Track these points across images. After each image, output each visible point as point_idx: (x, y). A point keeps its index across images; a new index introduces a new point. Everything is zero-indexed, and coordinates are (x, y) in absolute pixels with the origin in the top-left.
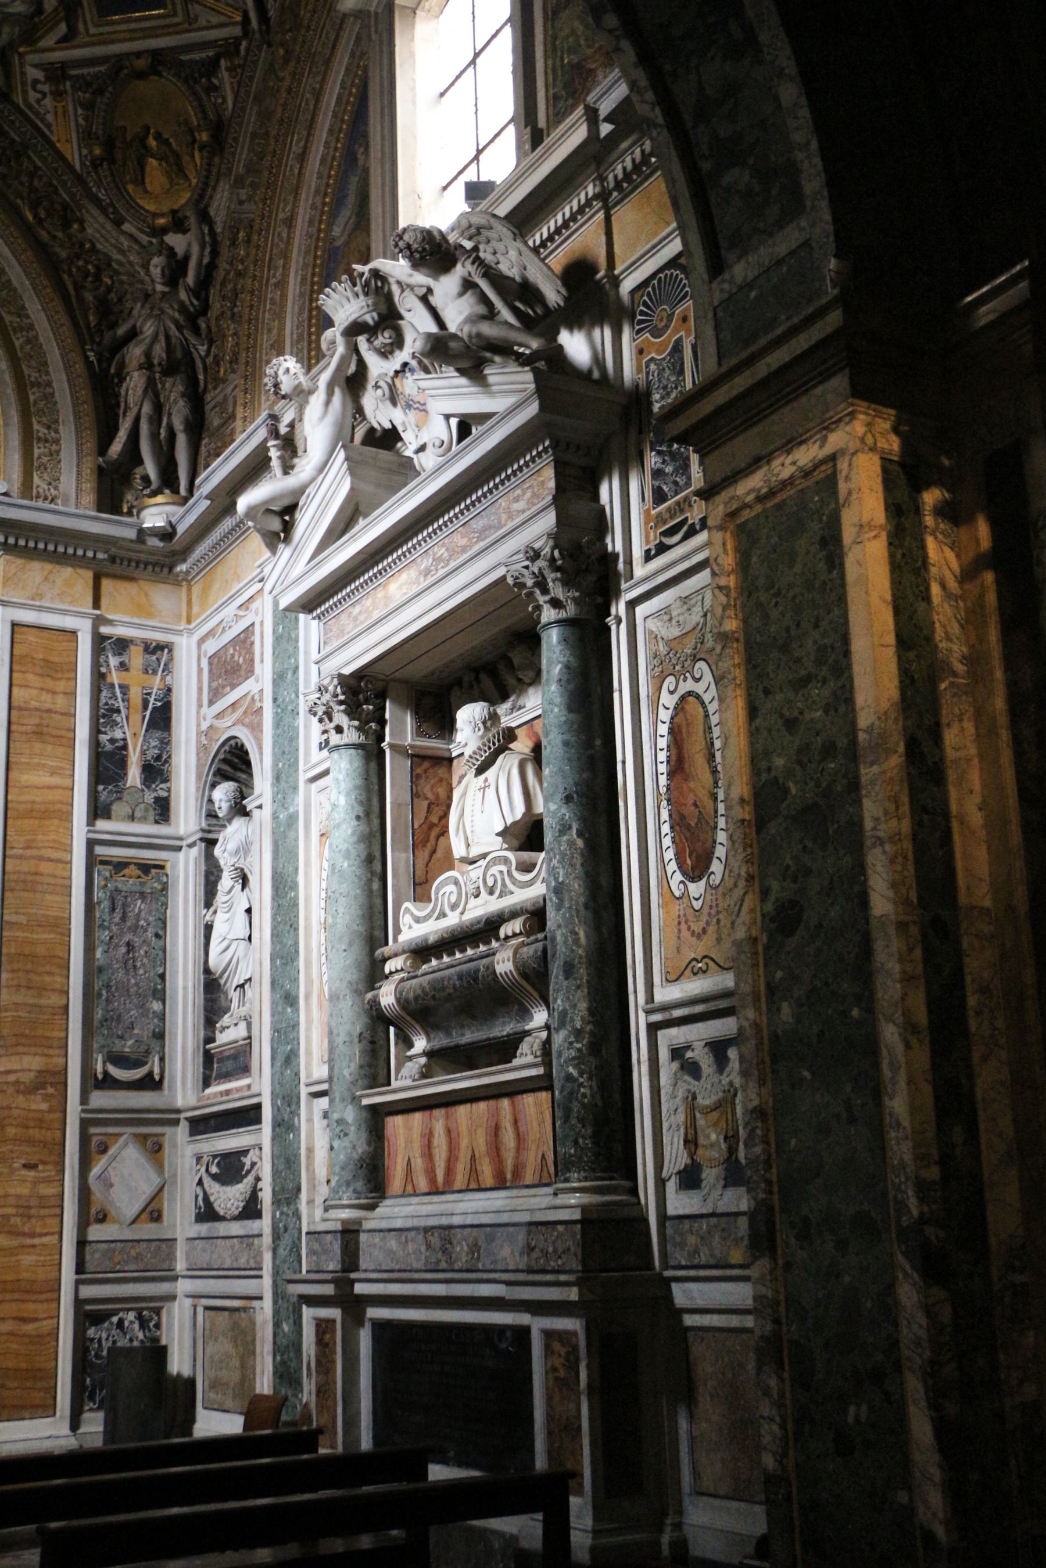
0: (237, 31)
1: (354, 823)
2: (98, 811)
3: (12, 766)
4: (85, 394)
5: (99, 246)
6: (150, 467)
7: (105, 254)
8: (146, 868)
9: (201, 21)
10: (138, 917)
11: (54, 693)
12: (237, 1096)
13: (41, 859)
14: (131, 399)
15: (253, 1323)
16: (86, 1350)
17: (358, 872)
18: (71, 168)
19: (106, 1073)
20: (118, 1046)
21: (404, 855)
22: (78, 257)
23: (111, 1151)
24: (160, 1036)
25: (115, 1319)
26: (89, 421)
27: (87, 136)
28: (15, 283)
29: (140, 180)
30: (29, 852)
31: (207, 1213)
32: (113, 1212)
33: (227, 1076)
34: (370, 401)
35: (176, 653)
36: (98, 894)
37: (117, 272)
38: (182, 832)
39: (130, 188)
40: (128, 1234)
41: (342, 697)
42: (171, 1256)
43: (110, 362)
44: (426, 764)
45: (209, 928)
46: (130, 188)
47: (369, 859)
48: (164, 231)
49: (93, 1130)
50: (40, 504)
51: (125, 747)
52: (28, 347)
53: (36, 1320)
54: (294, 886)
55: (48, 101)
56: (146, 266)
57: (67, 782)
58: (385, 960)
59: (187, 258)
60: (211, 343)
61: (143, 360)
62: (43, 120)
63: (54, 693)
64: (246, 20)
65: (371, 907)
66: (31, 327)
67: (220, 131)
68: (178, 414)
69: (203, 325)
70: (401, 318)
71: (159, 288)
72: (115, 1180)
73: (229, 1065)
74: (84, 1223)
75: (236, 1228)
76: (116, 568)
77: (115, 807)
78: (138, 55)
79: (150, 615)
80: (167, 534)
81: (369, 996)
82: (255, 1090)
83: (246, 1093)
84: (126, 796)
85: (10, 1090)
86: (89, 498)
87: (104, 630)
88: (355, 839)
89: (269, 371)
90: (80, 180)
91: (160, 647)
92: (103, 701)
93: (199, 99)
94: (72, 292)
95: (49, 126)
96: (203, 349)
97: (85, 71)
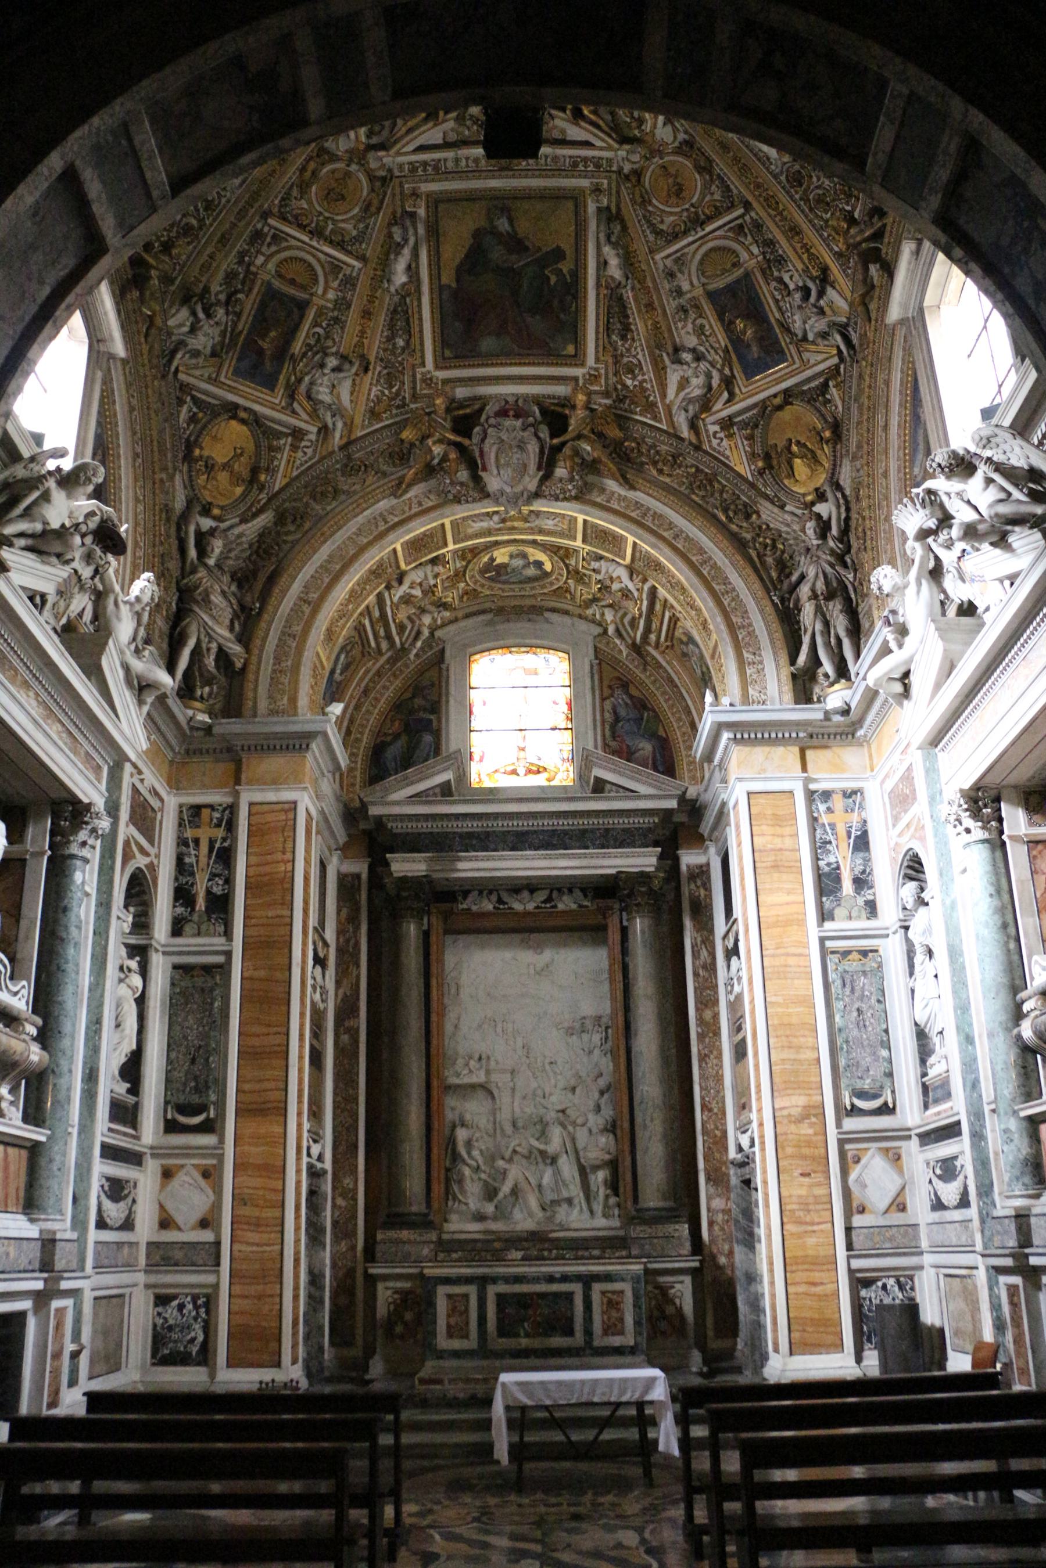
0: (836, 360)
1: (989, 900)
2: (824, 916)
3: (760, 892)
4: (776, 625)
6: (828, 667)
7: (777, 530)
8: (864, 953)
9: (812, 362)
10: (863, 989)
11: (782, 836)
12: (943, 1115)
13: (787, 955)
14: (807, 623)
15: (975, 1287)
16: (861, 1306)
17: (997, 937)
18: (746, 480)
19: (853, 1105)
20: (859, 1085)
21: (1031, 920)
22: (758, 535)
23: (863, 1162)
24: (890, 1075)
25: (880, 1284)
26: (780, 643)
27: (752, 456)
28: (719, 563)
29: (791, 474)
30: (779, 951)
31: (938, 1205)
32: (868, 1206)
33: (937, 1101)
34: (949, 582)
35: (866, 794)
36: (832, 976)
37: (786, 540)
38: (887, 924)
39: (786, 482)
40: (882, 1222)
41: (965, 806)
42: (916, 1237)
43: (789, 600)
44: (1040, 847)
45: (913, 991)
46: (786, 482)
47: (1005, 926)
48: (813, 504)
49: (848, 1147)
50: (755, 707)
51: (838, 868)
53: (822, 1284)
54: (961, 955)
55: (725, 443)
56: (803, 530)
57: (800, 899)
58: (1023, 1002)
59: (830, 518)
60: (855, 571)
61: (810, 593)
63: (782, 836)
64: (840, 352)
65: (1010, 963)
66: (734, 589)
67: (837, 428)
68: (840, 624)
69: (849, 561)
70: (953, 518)
71: (815, 542)
72: (868, 1182)
73: (940, 1093)
74: (848, 1213)
75: (957, 1215)
76: (815, 742)
77: (837, 912)
78: (775, 396)
79: (843, 771)
80: (846, 712)
81: (1015, 1031)
82: (955, 1110)
83: (950, 1113)
84: (843, 903)
85: (785, 1121)
86: (788, 696)
87: (813, 787)
88: (991, 911)
89: (873, 579)
90: (752, 485)
91: (854, 792)
92: (818, 836)
93: (819, 411)
94: (756, 559)
95: (727, 458)
96: (851, 577)
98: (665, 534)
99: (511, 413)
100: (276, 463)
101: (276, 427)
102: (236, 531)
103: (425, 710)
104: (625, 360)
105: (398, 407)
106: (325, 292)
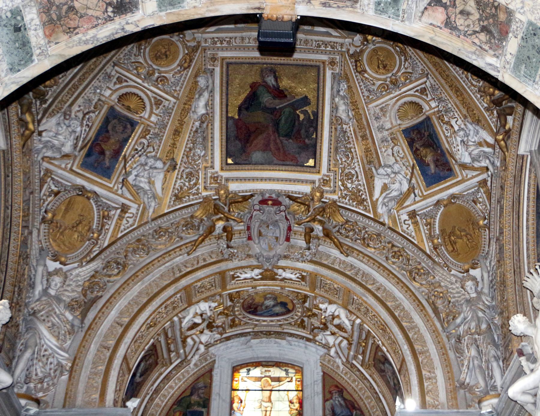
5: (442, 284)
7: (446, 286)
28: (406, 308)
52: (416, 336)
62: (410, 236)
97: (425, 211)
98: (370, 287)
99: (270, 202)
100: (107, 227)
101: (109, 203)
102: (77, 271)
103: (199, 405)
104: (347, 171)
105: (194, 195)
106: (150, 116)
